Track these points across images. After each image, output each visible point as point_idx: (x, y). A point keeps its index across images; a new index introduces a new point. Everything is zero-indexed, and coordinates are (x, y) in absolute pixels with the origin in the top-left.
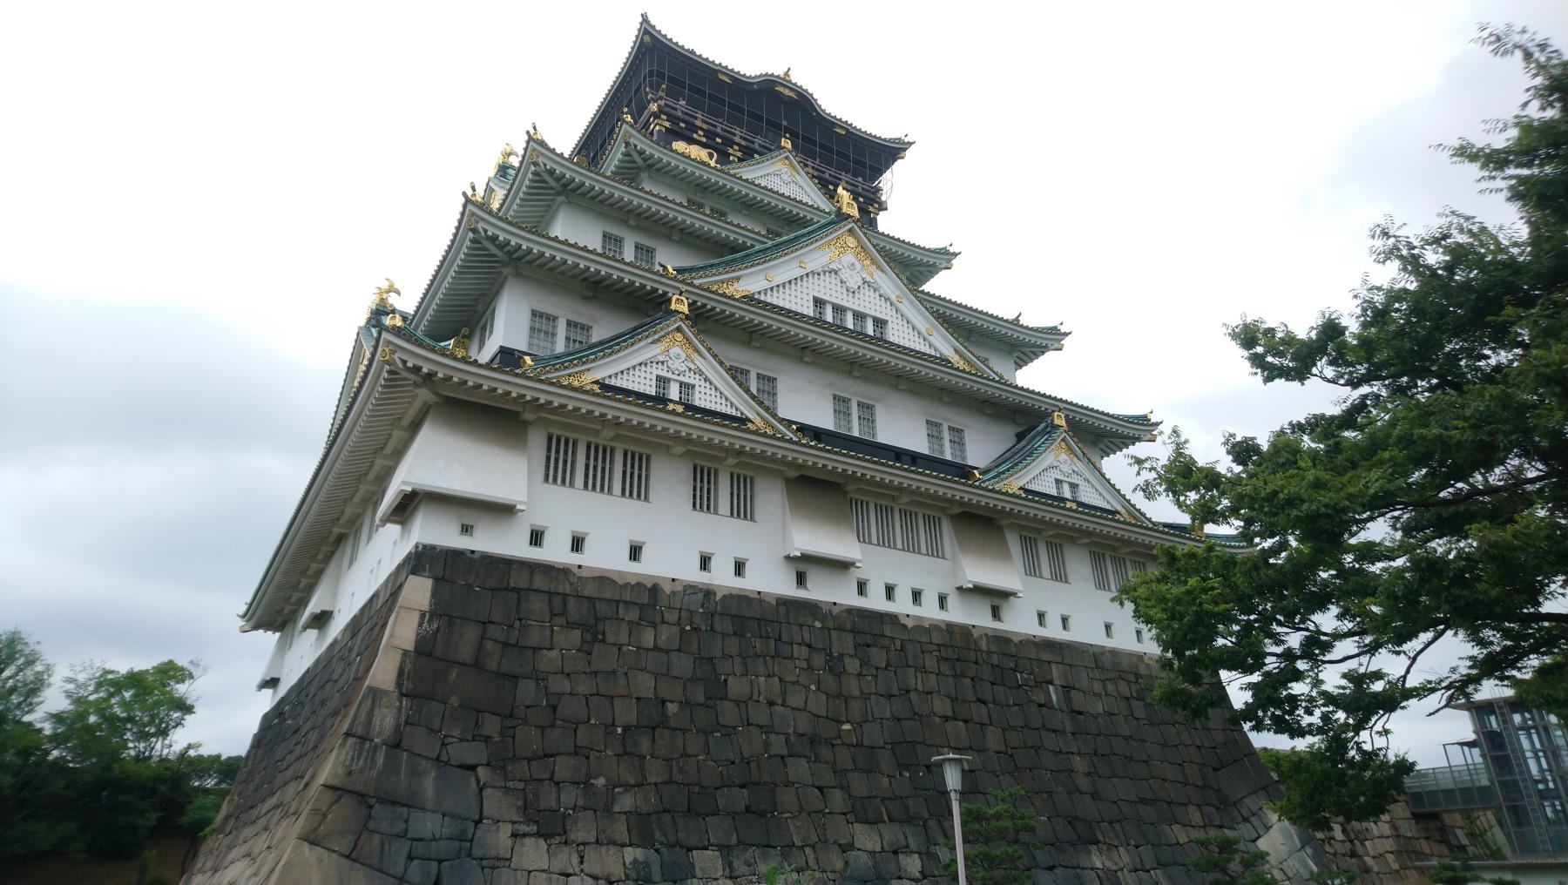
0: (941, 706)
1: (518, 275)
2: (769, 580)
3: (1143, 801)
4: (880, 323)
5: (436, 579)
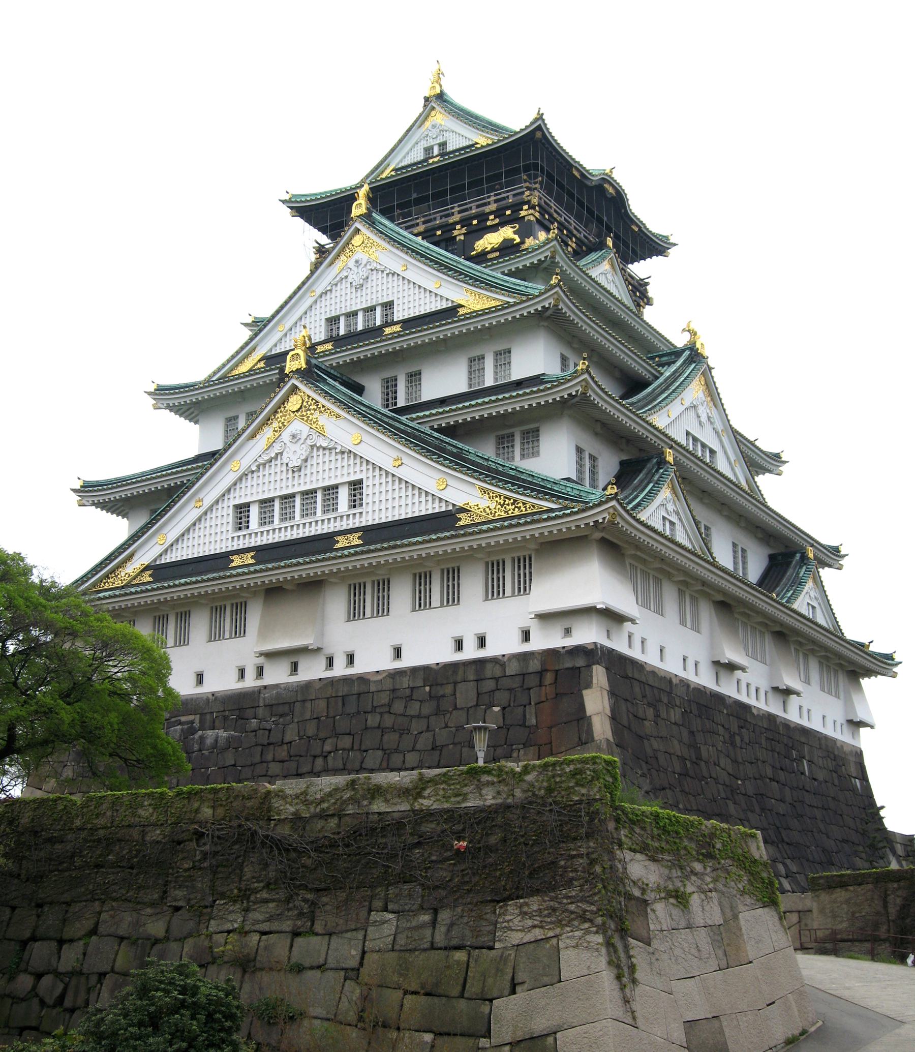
0: (769, 772)
1: (570, 416)
2: (705, 679)
3: (843, 841)
4: (712, 452)
5: (607, 669)
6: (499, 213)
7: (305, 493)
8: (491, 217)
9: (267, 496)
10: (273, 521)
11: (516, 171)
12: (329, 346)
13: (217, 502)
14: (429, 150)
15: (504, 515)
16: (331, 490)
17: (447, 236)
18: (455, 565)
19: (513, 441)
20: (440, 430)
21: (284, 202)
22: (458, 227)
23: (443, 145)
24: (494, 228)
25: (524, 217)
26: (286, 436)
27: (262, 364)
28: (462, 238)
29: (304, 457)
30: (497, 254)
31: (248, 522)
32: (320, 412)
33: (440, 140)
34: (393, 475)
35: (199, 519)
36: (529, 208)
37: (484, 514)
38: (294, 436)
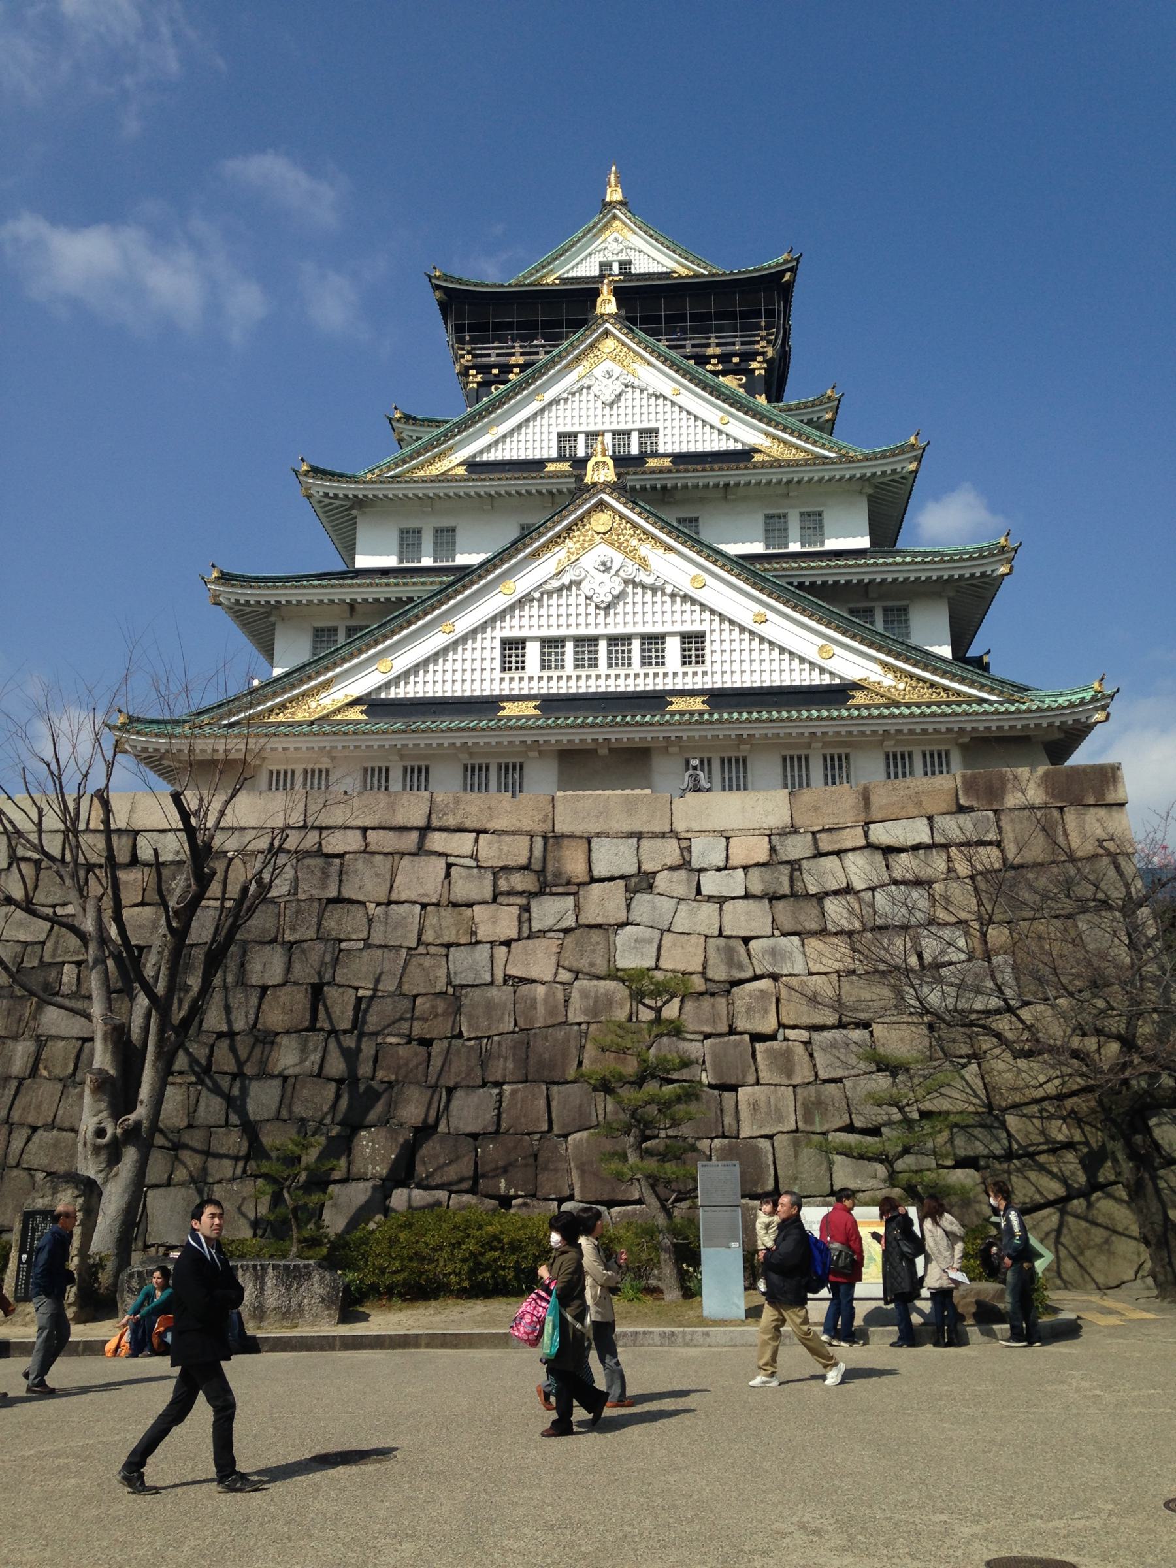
6: (724, 358)
7: (613, 640)
8: (714, 361)
9: (554, 632)
10: (563, 667)
12: (565, 467)
13: (474, 631)
14: (605, 265)
15: (915, 699)
16: (654, 641)
18: (843, 751)
19: (873, 616)
20: (800, 586)
21: (430, 277)
25: (754, 370)
26: (589, 561)
27: (461, 471)
29: (616, 593)
31: (523, 662)
32: (640, 540)
33: (623, 257)
34: (751, 633)
35: (445, 651)
36: (765, 361)
37: (889, 695)
38: (603, 564)
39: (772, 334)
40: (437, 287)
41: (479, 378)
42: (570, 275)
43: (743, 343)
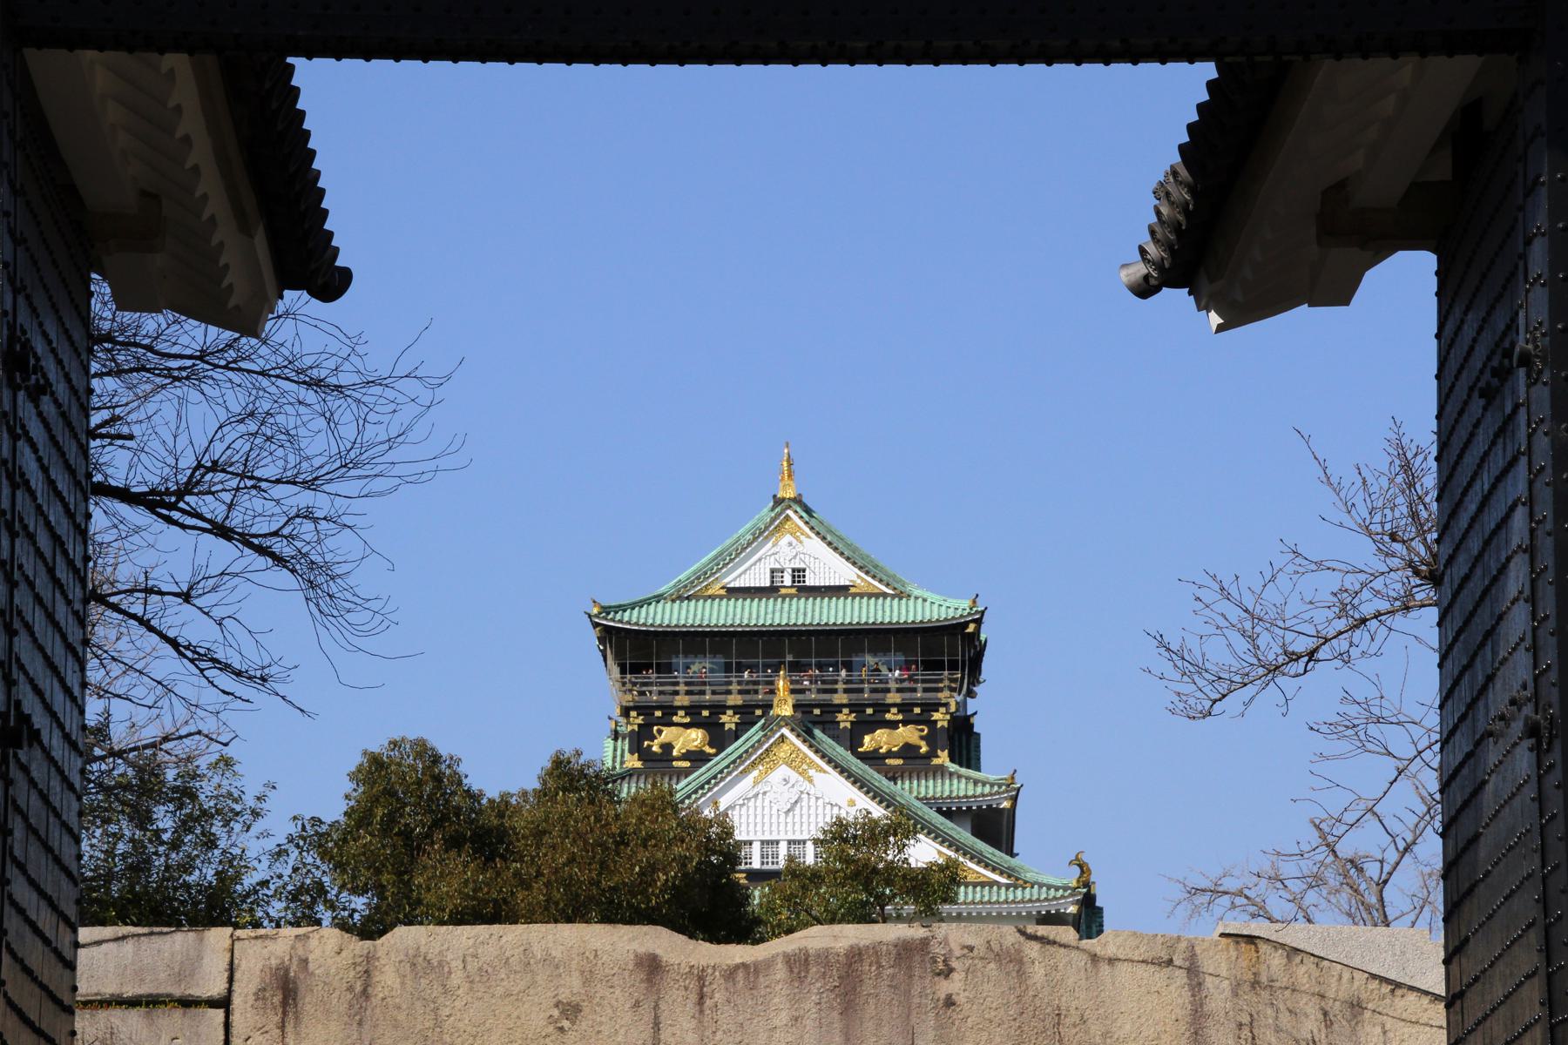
6: (904, 708)
8: (894, 710)
11: (939, 666)
17: (828, 717)
22: (846, 711)
23: (798, 573)
24: (893, 725)
28: (848, 725)
30: (900, 762)
39: (955, 680)
40: (596, 625)
41: (640, 720)
42: (737, 585)
43: (925, 690)
